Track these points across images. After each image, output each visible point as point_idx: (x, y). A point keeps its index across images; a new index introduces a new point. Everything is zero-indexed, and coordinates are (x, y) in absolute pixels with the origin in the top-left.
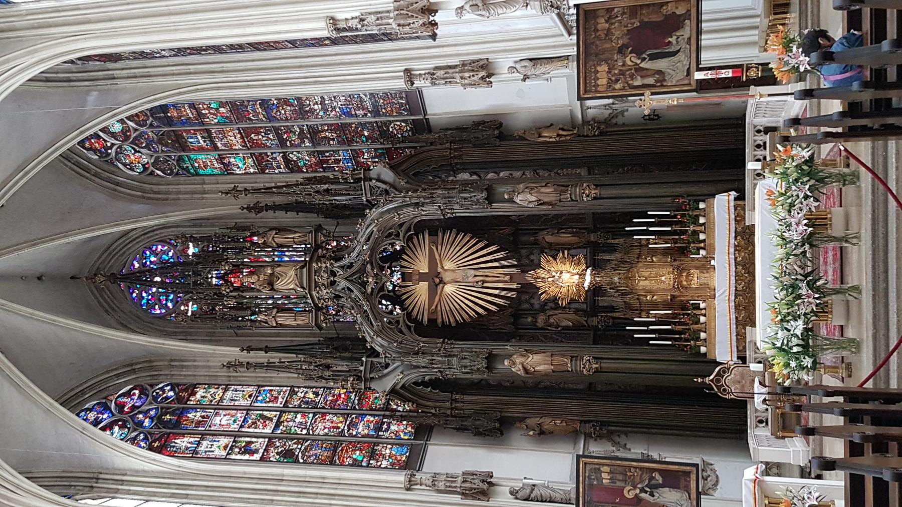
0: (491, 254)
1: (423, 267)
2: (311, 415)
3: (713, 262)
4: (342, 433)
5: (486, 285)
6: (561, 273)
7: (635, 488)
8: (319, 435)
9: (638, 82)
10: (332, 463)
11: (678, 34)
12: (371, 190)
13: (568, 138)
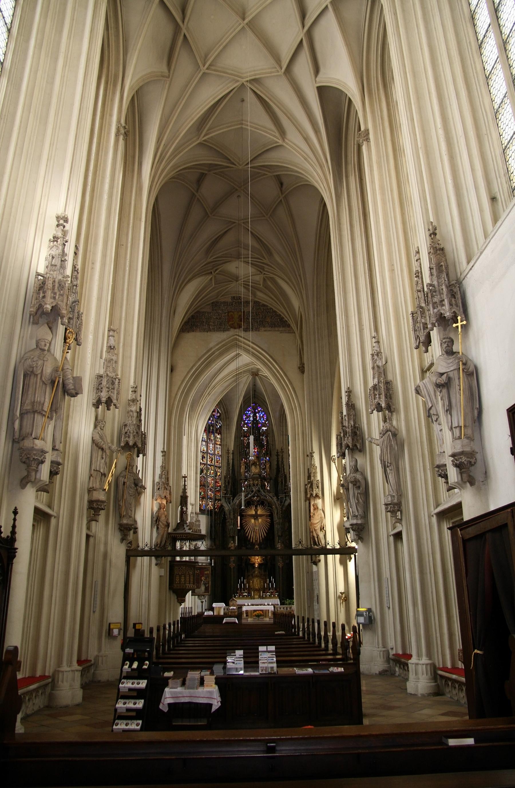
0: (263, 534)
4: (208, 487)
10: (200, 486)
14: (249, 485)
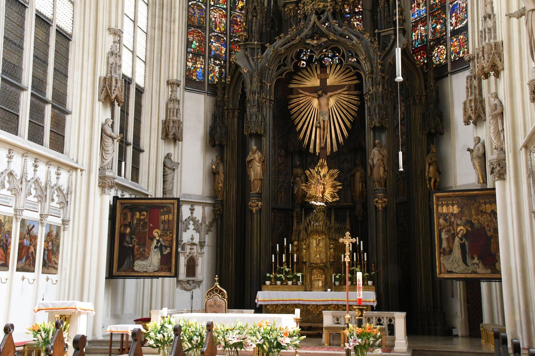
1: (331, 81)
2: (225, 6)
3: (329, 290)
4: (211, 31)
5: (318, 130)
6: (323, 184)
7: (160, 236)
8: (210, 14)
9: (444, 236)
10: (189, 26)
11: (480, 264)
12: (387, 35)
13: (428, 186)
14: (304, 14)
